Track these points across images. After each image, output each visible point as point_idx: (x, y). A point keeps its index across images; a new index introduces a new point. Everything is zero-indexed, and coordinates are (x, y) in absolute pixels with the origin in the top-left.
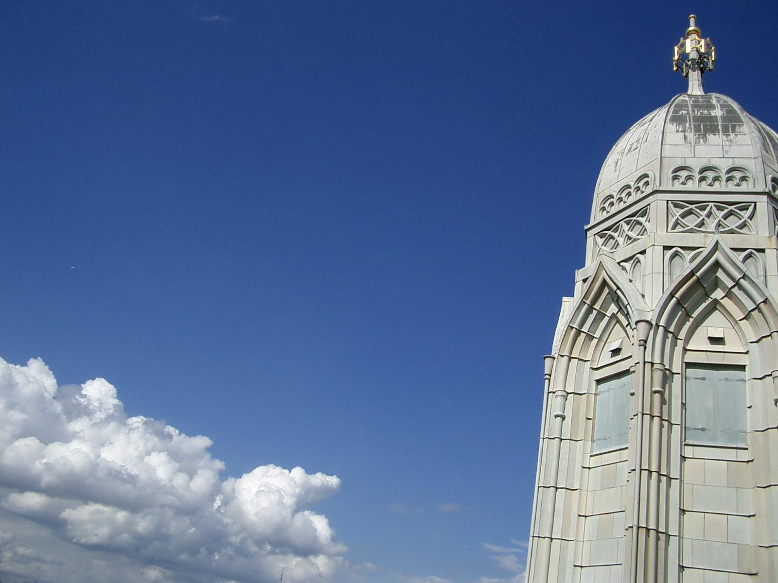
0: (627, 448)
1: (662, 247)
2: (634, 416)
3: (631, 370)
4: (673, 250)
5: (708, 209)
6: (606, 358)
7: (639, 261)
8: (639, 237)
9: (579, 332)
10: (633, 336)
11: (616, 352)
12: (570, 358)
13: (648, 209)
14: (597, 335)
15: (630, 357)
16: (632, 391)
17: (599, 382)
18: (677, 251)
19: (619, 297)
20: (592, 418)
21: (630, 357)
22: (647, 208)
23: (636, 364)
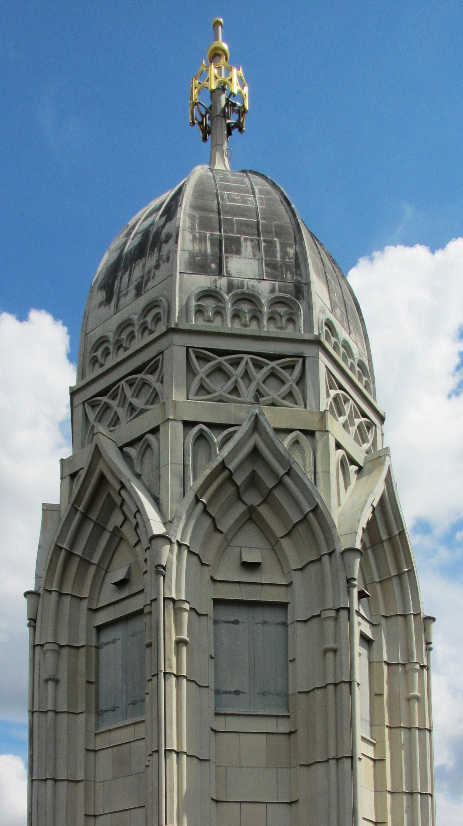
0: (143, 721)
1: (181, 425)
2: (153, 676)
3: (147, 610)
4: (196, 429)
5: (242, 364)
6: (108, 594)
7: (149, 446)
8: (149, 407)
9: (70, 554)
10: (146, 561)
11: (121, 584)
12: (61, 594)
13: (160, 362)
14: (96, 560)
15: (142, 591)
16: (148, 641)
17: (100, 629)
18: (201, 430)
19: (123, 501)
20: (94, 681)
21: (142, 591)
22: (159, 360)
23: (152, 601)
